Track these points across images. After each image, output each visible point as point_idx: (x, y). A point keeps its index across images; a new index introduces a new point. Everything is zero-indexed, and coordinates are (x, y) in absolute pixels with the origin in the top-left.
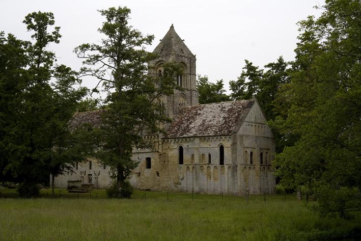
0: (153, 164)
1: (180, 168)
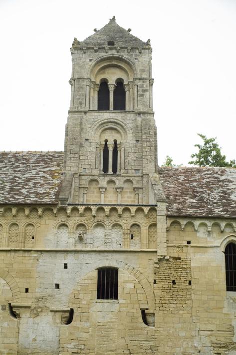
0: (131, 286)
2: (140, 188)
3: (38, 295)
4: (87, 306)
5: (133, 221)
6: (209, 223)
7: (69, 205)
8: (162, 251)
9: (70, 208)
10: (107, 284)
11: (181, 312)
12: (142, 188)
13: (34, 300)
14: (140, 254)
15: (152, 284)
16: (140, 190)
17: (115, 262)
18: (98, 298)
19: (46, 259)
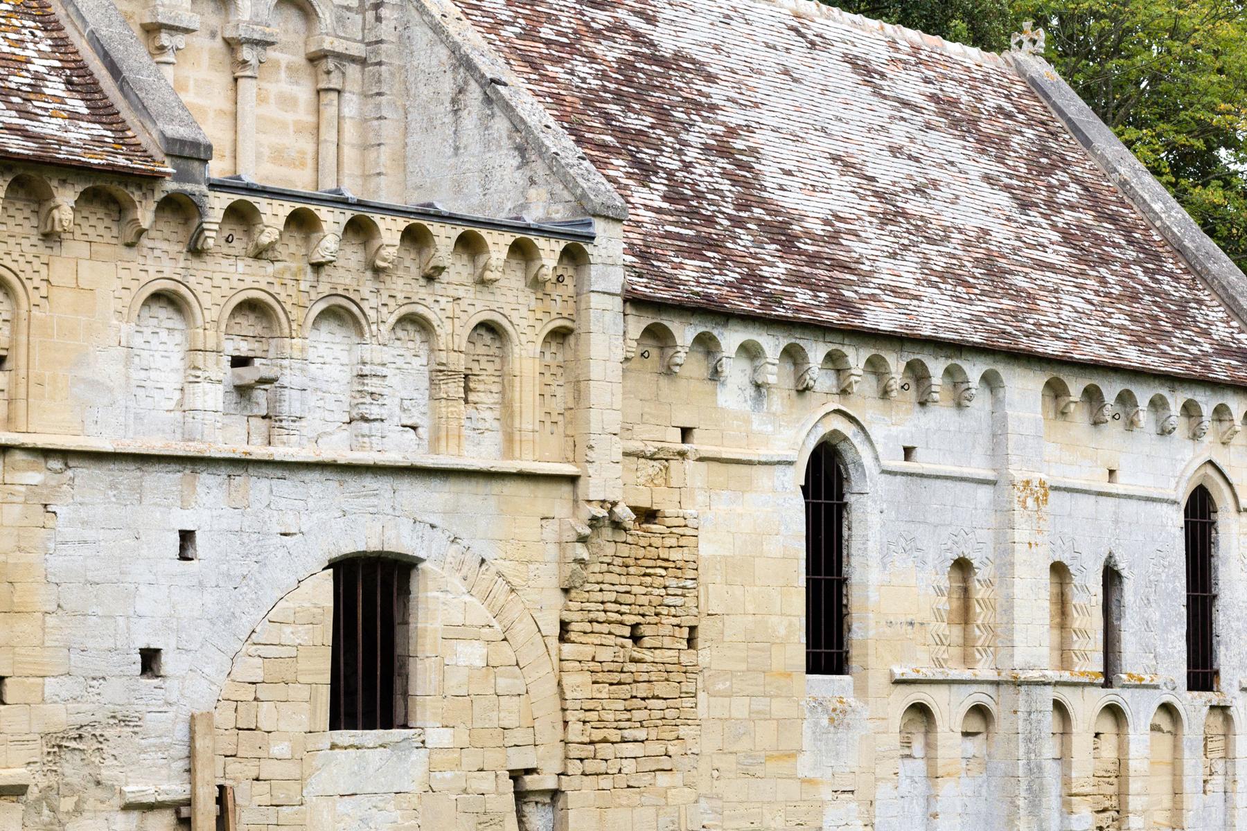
0: (471, 654)
1: (838, 717)
2: (353, 59)
3: (60, 717)
4: (293, 770)
5: (479, 308)
6: (772, 344)
7: (214, 186)
8: (610, 482)
9: (218, 203)
10: (369, 641)
11: (663, 780)
12: (363, 62)
13: (37, 750)
14: (510, 488)
15: (553, 642)
16: (353, 70)
17: (406, 526)
18: (334, 726)
19: (89, 497)
